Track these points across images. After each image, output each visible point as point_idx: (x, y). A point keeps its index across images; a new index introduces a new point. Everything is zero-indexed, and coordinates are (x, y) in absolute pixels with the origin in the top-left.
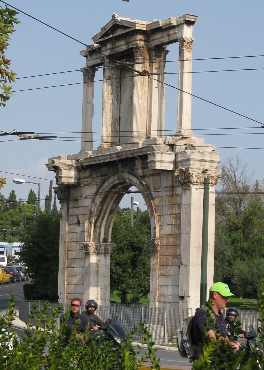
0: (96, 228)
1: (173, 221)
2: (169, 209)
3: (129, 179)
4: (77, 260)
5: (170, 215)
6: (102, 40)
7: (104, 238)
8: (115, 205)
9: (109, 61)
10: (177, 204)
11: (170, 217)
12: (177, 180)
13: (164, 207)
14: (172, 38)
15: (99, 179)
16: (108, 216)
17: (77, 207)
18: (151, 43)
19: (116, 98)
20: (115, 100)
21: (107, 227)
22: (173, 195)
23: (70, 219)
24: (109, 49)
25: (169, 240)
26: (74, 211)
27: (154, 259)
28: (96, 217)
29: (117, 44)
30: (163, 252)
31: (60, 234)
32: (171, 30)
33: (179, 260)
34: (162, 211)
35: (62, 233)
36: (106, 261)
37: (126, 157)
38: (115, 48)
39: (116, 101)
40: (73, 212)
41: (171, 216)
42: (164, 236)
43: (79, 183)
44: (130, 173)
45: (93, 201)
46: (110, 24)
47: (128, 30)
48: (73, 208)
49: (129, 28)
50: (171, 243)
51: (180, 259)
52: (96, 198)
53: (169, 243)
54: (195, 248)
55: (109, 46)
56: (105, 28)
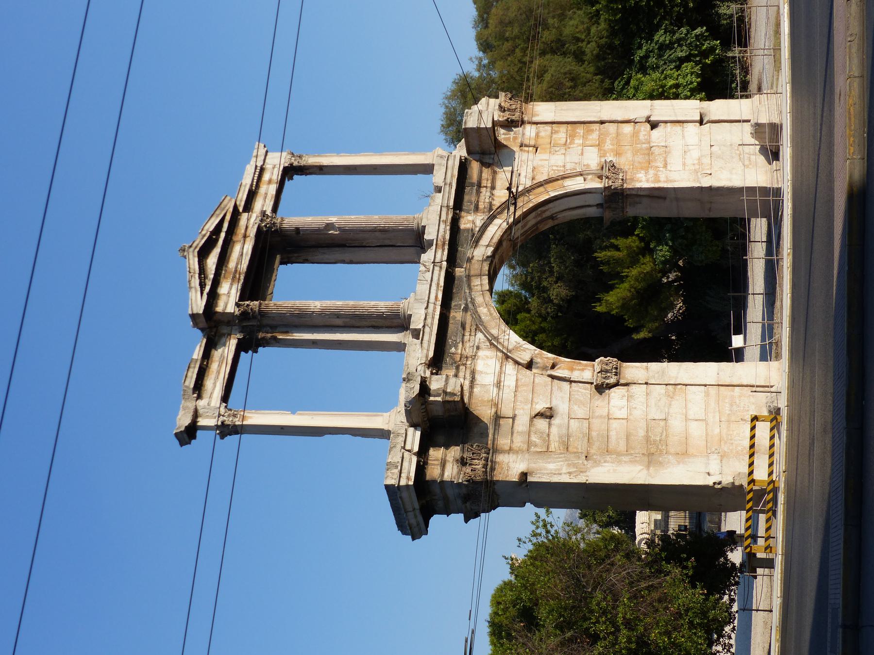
1: (577, 144)
2: (556, 151)
3: (487, 246)
4: (631, 414)
5: (568, 150)
6: (207, 289)
13: (552, 162)
17: (514, 418)
23: (536, 446)
25: (608, 149)
27: (637, 181)
29: (232, 265)
32: (263, 179)
33: (642, 129)
34: (557, 166)
35: (565, 470)
37: (448, 228)
41: (569, 148)
44: (477, 242)
47: (228, 217)
50: (613, 145)
53: (612, 150)
56: (192, 277)
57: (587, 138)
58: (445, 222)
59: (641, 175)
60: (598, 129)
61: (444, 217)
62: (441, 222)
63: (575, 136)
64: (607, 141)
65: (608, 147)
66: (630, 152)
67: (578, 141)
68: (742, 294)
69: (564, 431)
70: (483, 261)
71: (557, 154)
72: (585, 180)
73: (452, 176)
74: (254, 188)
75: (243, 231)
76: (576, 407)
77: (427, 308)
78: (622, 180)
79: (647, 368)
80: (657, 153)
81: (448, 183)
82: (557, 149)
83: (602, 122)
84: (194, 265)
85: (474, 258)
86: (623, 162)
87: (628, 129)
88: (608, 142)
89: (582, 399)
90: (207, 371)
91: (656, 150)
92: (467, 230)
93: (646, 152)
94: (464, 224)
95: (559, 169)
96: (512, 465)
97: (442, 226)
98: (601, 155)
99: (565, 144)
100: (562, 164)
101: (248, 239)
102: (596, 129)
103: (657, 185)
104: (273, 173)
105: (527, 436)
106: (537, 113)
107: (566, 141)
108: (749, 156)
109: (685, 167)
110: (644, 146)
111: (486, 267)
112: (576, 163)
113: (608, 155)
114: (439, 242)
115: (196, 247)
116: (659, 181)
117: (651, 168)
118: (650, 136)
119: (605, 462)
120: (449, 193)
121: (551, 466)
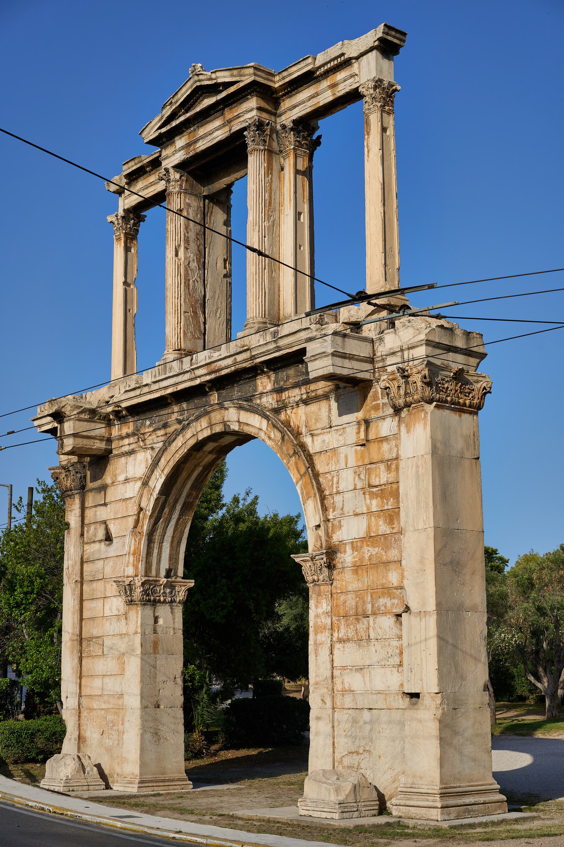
0: (152, 545)
2: (359, 475)
3: (239, 422)
4: (107, 620)
6: (164, 130)
7: (169, 567)
8: (194, 493)
9: (180, 178)
10: (382, 462)
11: (363, 496)
12: (378, 402)
13: (343, 474)
14: (343, 89)
15: (160, 435)
16: (179, 519)
17: (105, 504)
18: (283, 118)
19: (195, 258)
20: (193, 260)
21: (175, 543)
22: (368, 441)
23: (88, 532)
24: (183, 148)
25: (364, 553)
26: (98, 513)
27: (317, 602)
28: (152, 521)
29: (201, 131)
30: (344, 583)
31: (65, 566)
33: (396, 601)
34: (338, 483)
35: (70, 562)
36: (174, 619)
37: (233, 368)
38: (196, 142)
39: (197, 262)
40: (95, 515)
41: (364, 494)
42: (345, 544)
43: (110, 451)
44: (241, 408)
45: (145, 484)
46: (184, 89)
47: (232, 89)
48: (96, 506)
49: (233, 83)
51: (402, 599)
52: (153, 477)
53: (362, 559)
54: (444, 565)
55: (180, 142)
57: (379, 517)
59: (325, 606)
60: (394, 531)
62: (233, 358)
63: (382, 498)
64: (376, 549)
65: (366, 552)
66: (360, 585)
67: (375, 505)
69: (96, 557)
70: (224, 423)
71: (354, 478)
72: (318, 526)
73: (290, 346)
74: (318, 73)
75: (236, 114)
76: (111, 563)
77: (155, 382)
78: (314, 581)
79: (136, 633)
80: (358, 627)
81: (278, 345)
82: (362, 476)
84: (182, 95)
85: (226, 411)
88: (374, 551)
89: (117, 568)
90: (145, 176)
91: (361, 626)
93: (360, 610)
94: (261, 383)
95: (335, 486)
96: (74, 512)
97: (229, 361)
98: (355, 544)
99: (370, 486)
100: (341, 489)
101: (227, 129)
102: (393, 528)
103: (311, 630)
104: (345, 81)
105: (93, 522)
106: (412, 429)
107: (376, 486)
108: (356, 766)
109: (339, 669)
111: (218, 429)
112: (342, 509)
113: (356, 553)
114: (213, 365)
115: (199, 81)
116: (316, 634)
117: (337, 620)
118: (384, 614)
119: (74, 599)
121: (72, 550)
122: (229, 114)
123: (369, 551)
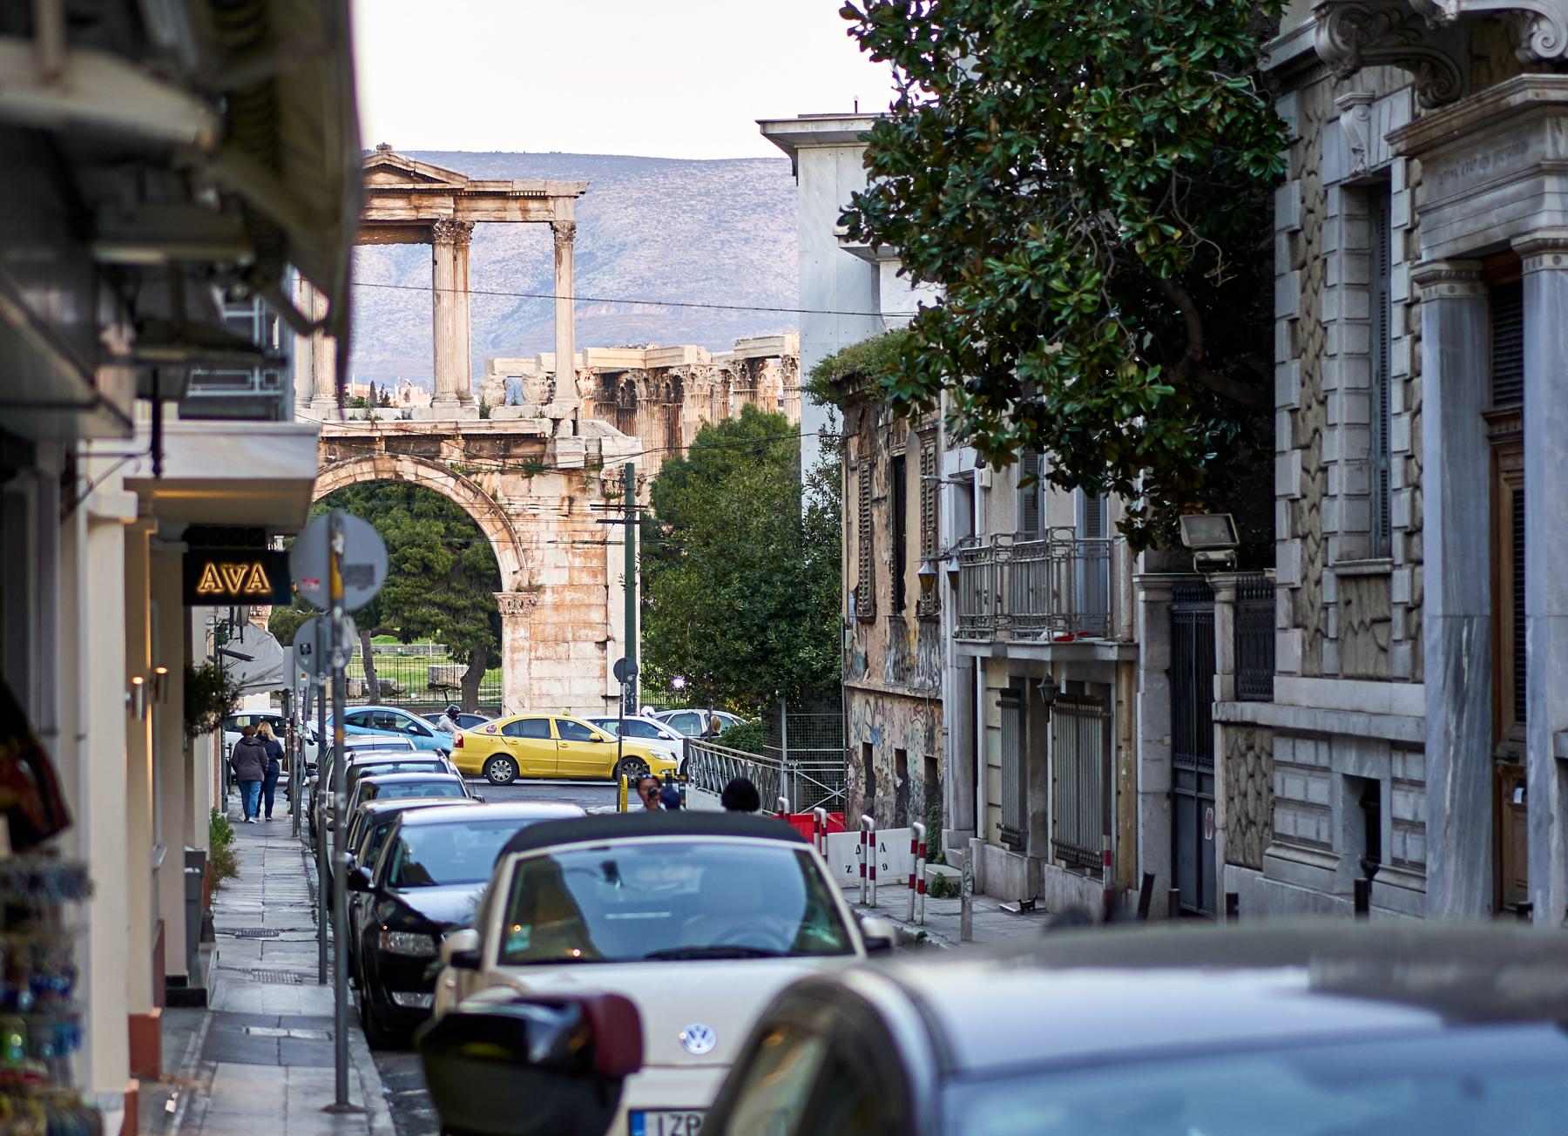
3: (416, 475)
44: (421, 463)
47: (436, 186)
50: (572, 600)
53: (563, 601)
58: (436, 427)
59: (522, 632)
61: (440, 426)
67: (578, 562)
68: (784, 750)
70: (396, 473)
72: (515, 572)
73: (505, 429)
75: (425, 203)
83: (607, 587)
86: (547, 616)
87: (596, 616)
88: (576, 595)
91: (562, 648)
92: (439, 451)
93: (560, 638)
97: (428, 426)
110: (569, 636)
120: (479, 428)
122: (415, 201)
123: (569, 596)
